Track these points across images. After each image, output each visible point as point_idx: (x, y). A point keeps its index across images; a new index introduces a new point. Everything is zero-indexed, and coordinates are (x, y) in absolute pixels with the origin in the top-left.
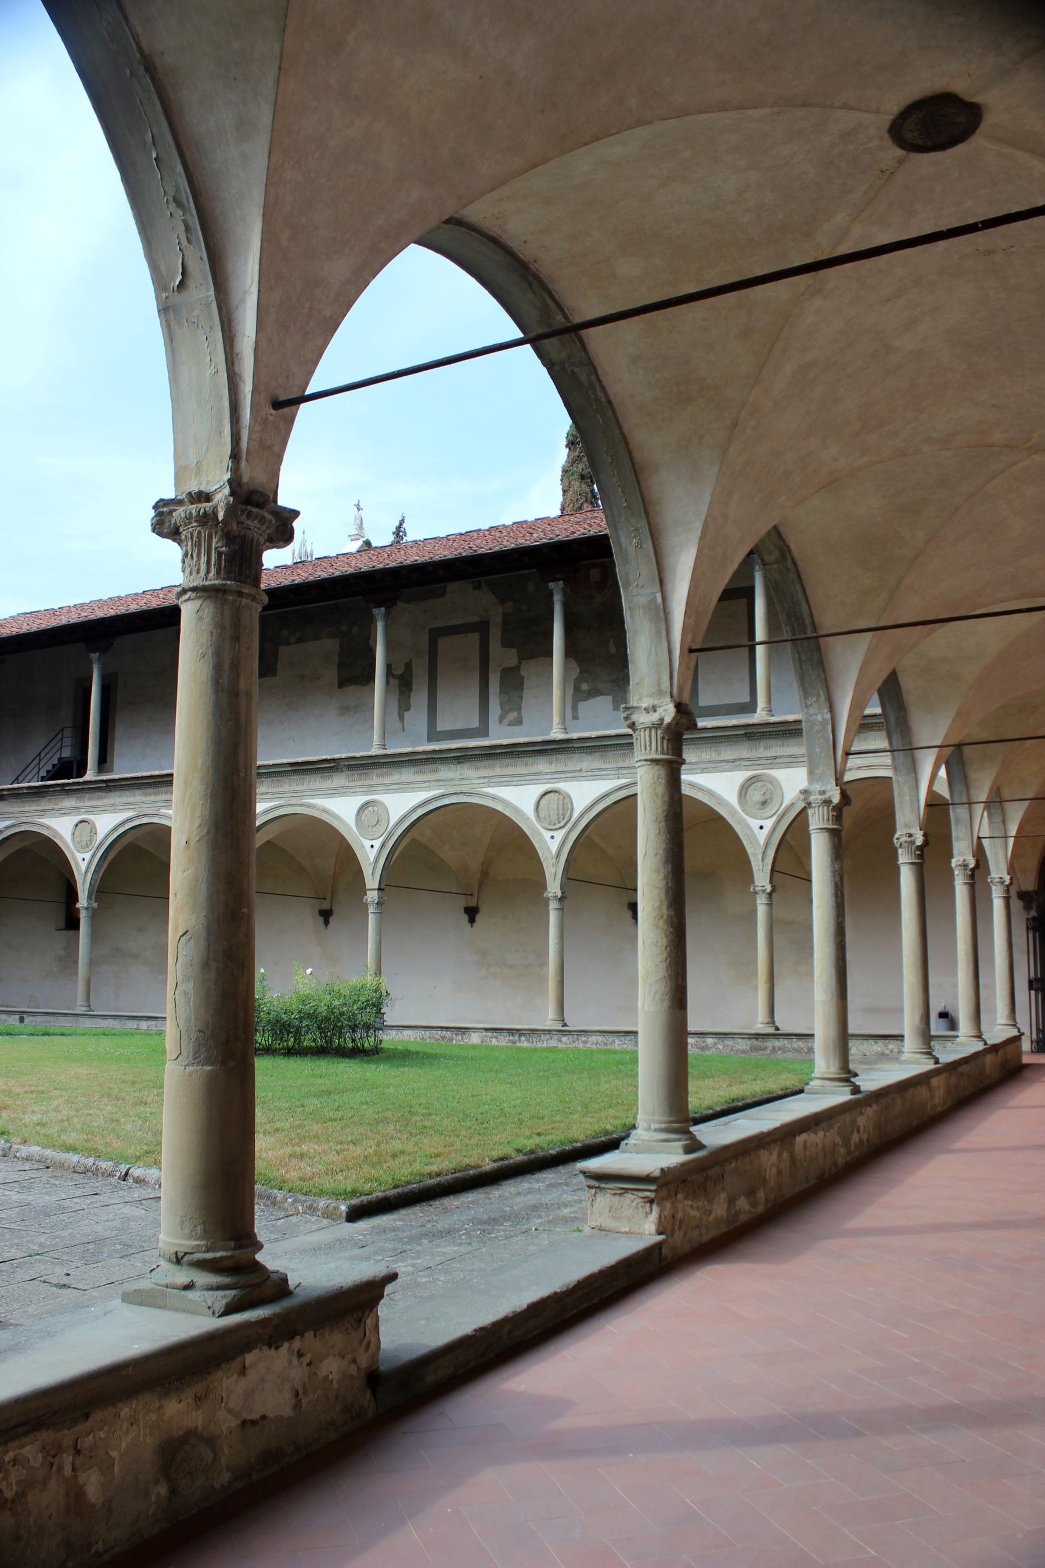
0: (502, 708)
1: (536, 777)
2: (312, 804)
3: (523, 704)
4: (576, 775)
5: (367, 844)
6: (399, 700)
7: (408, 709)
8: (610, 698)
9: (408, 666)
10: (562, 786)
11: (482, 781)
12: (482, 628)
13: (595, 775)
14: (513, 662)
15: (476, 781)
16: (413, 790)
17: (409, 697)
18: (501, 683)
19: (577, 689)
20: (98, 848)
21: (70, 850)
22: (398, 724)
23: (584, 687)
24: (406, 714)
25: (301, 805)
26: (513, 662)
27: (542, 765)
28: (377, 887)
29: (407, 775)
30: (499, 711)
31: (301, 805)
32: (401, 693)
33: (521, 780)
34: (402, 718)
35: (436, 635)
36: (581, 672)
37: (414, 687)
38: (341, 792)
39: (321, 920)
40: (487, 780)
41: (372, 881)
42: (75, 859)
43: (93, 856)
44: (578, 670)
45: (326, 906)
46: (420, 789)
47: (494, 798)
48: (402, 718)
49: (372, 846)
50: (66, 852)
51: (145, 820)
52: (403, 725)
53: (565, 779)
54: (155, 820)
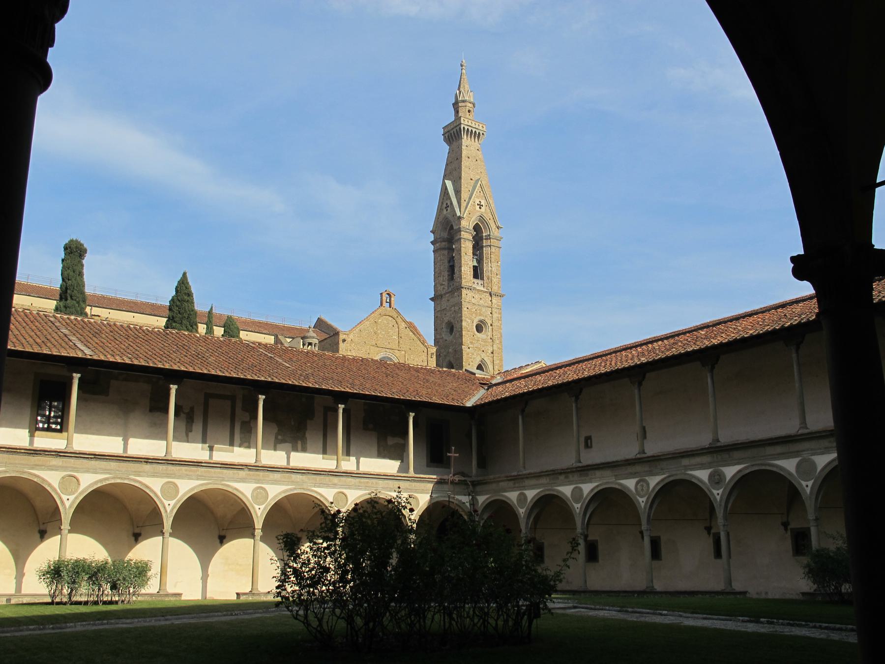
0: (241, 440)
1: (334, 486)
2: (229, 485)
3: (252, 440)
4: (349, 487)
5: (257, 507)
6: (186, 425)
7: (191, 431)
8: (290, 445)
9: (192, 409)
10: (344, 491)
11: (311, 484)
12: (233, 399)
13: (357, 487)
14: (248, 419)
15: (309, 484)
16: (280, 484)
17: (192, 426)
18: (241, 428)
19: (276, 438)
20: (80, 494)
21: (57, 493)
22: (185, 438)
23: (280, 437)
24: (190, 434)
25: (222, 485)
26: (248, 419)
27: (335, 480)
28: (261, 528)
29: (277, 476)
30: (239, 442)
31: (222, 485)
32: (188, 422)
33: (327, 486)
34: (187, 435)
35: (208, 396)
36: (278, 430)
37: (195, 421)
38: (243, 480)
39: (133, 539)
40: (314, 485)
41: (259, 524)
42: (60, 498)
43: (76, 498)
44: (277, 429)
45: (137, 531)
46: (283, 485)
47: (316, 492)
48: (187, 435)
49: (259, 509)
50: (53, 494)
51: (119, 481)
52: (188, 439)
53: (346, 488)
54: (126, 482)
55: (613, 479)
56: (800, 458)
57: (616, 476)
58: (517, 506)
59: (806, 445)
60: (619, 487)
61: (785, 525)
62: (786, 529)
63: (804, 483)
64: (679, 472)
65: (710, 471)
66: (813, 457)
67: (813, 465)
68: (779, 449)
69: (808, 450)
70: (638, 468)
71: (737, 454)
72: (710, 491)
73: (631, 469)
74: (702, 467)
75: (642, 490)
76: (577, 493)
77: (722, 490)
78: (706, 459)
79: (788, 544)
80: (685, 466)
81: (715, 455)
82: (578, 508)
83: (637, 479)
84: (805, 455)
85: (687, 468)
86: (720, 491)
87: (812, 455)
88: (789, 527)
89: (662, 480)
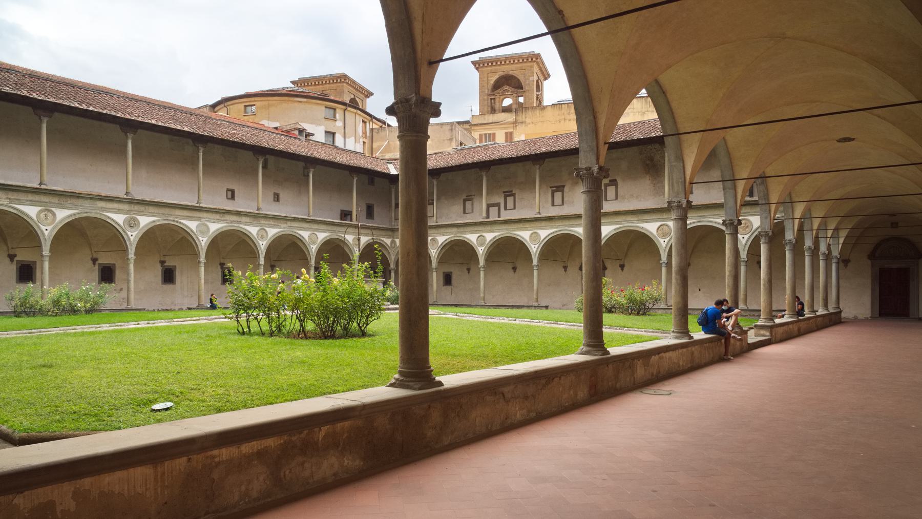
55: (6, 202)
56: (199, 222)
57: (10, 199)
58: (54, 224)
59: (205, 215)
60: (15, 212)
61: (94, 260)
62: (94, 264)
63: (201, 239)
64: (94, 211)
65: (125, 216)
66: (208, 223)
67: (208, 229)
68: (185, 213)
69: (206, 218)
70: (43, 198)
71: (152, 209)
72: (125, 232)
73: (31, 197)
74: (119, 211)
75: (46, 219)
76: (204, 230)
77: (136, 232)
78: (125, 207)
79: (96, 274)
80: (101, 208)
81: (133, 206)
82: (46, 230)
83: (40, 208)
84: (203, 221)
85: (103, 209)
86: (134, 234)
87: (209, 222)
88: (97, 263)
89: (74, 215)
